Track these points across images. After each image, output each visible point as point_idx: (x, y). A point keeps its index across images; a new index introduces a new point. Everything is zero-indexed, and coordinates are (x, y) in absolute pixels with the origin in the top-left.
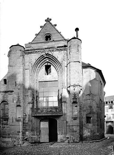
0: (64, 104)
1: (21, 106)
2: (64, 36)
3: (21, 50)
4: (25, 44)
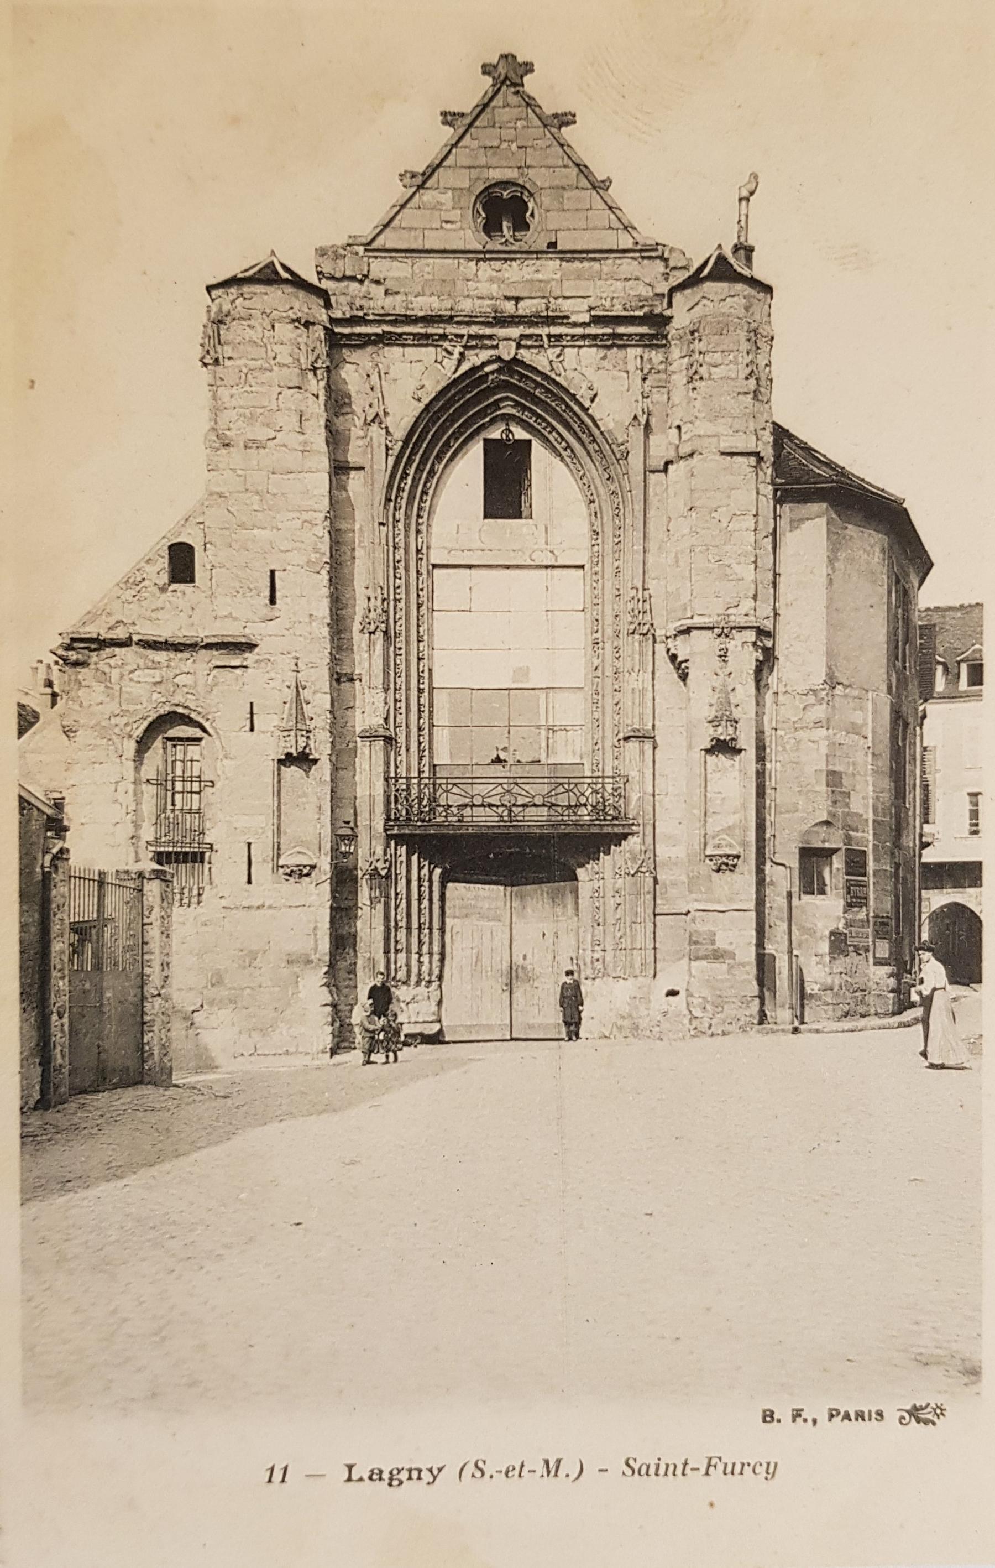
0: (642, 752)
1: (315, 761)
2: (630, 215)
3: (307, 324)
4: (322, 252)
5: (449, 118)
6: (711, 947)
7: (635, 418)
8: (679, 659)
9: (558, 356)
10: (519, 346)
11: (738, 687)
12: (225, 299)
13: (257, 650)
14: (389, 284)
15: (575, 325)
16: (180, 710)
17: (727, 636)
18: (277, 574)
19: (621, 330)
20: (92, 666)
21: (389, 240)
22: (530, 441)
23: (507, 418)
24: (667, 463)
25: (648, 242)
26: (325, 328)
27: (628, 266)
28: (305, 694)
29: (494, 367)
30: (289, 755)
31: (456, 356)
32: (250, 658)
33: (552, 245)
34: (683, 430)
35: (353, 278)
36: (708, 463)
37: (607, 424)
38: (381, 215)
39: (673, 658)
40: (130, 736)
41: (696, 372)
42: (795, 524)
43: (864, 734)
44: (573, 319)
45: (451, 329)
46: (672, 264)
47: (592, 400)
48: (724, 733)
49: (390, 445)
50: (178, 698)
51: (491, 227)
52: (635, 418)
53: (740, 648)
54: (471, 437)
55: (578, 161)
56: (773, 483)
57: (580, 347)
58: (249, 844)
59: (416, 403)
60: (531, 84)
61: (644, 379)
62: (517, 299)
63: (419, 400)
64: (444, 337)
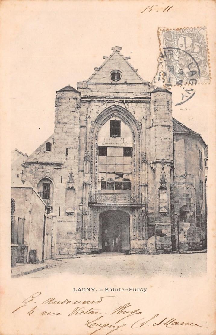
0: (145, 188)
1: (75, 189)
2: (142, 77)
6: (160, 233)
7: (143, 117)
8: (154, 168)
10: (119, 103)
11: (166, 175)
12: (60, 94)
13: (63, 165)
14: (91, 90)
15: (131, 99)
16: (47, 178)
17: (164, 164)
18: (68, 149)
19: (140, 100)
20: (29, 168)
21: (92, 81)
22: (120, 121)
24: (150, 127)
25: (146, 82)
26: (80, 100)
27: (141, 86)
28: (73, 175)
29: (114, 106)
31: (106, 104)
32: (62, 166)
33: (126, 82)
34: (154, 121)
35: (84, 88)
36: (159, 128)
37: (137, 119)
38: (90, 76)
39: (152, 168)
40: (36, 183)
41: (157, 109)
42: (177, 140)
43: (193, 185)
44: (131, 97)
45: (105, 99)
46: (150, 86)
47: (134, 114)
48: (163, 185)
49: (92, 122)
50: (47, 175)
51: (113, 78)
52: (143, 117)
53: (166, 167)
55: (131, 66)
56: (173, 132)
57: (132, 103)
58: (60, 207)
59: (97, 114)
60: (121, 52)
61: (145, 109)
62: (118, 93)
63: (98, 113)
64: (104, 101)
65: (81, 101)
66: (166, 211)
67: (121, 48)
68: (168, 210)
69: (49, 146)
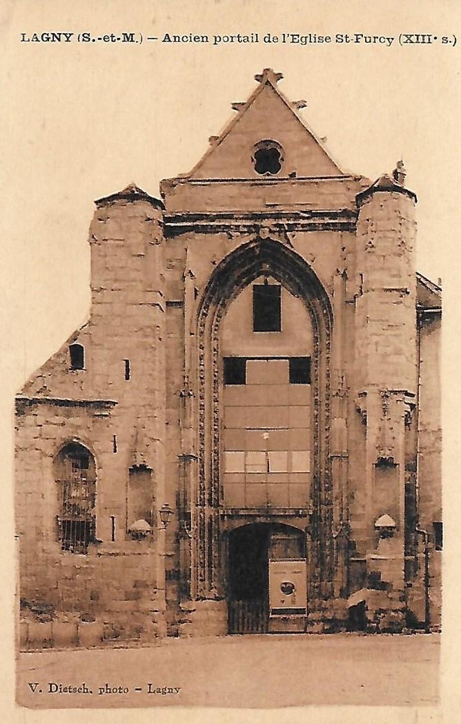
1: (150, 470)
5: (235, 106)
9: (294, 236)
16: (75, 440)
23: (267, 274)
30: (134, 466)
54: (247, 283)
56: (417, 308)
64: (228, 227)
65: (170, 233)
66: (393, 524)
67: (279, 76)
68: (396, 518)
69: (76, 355)
